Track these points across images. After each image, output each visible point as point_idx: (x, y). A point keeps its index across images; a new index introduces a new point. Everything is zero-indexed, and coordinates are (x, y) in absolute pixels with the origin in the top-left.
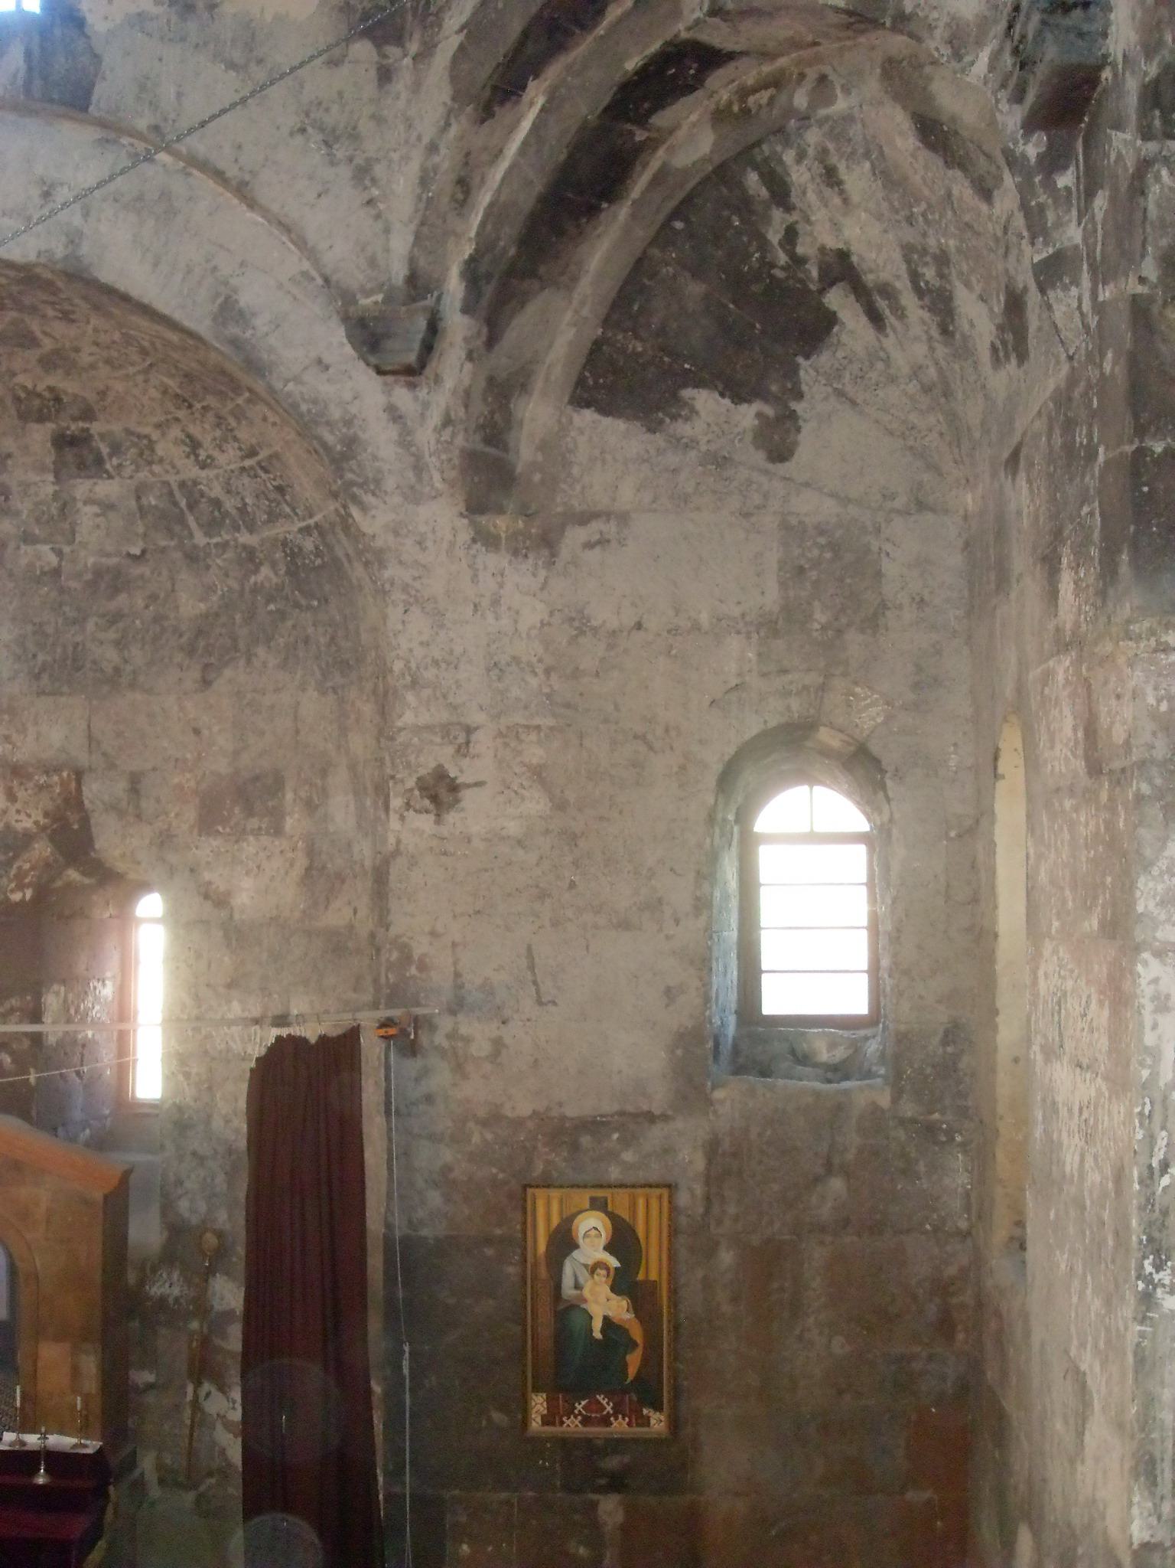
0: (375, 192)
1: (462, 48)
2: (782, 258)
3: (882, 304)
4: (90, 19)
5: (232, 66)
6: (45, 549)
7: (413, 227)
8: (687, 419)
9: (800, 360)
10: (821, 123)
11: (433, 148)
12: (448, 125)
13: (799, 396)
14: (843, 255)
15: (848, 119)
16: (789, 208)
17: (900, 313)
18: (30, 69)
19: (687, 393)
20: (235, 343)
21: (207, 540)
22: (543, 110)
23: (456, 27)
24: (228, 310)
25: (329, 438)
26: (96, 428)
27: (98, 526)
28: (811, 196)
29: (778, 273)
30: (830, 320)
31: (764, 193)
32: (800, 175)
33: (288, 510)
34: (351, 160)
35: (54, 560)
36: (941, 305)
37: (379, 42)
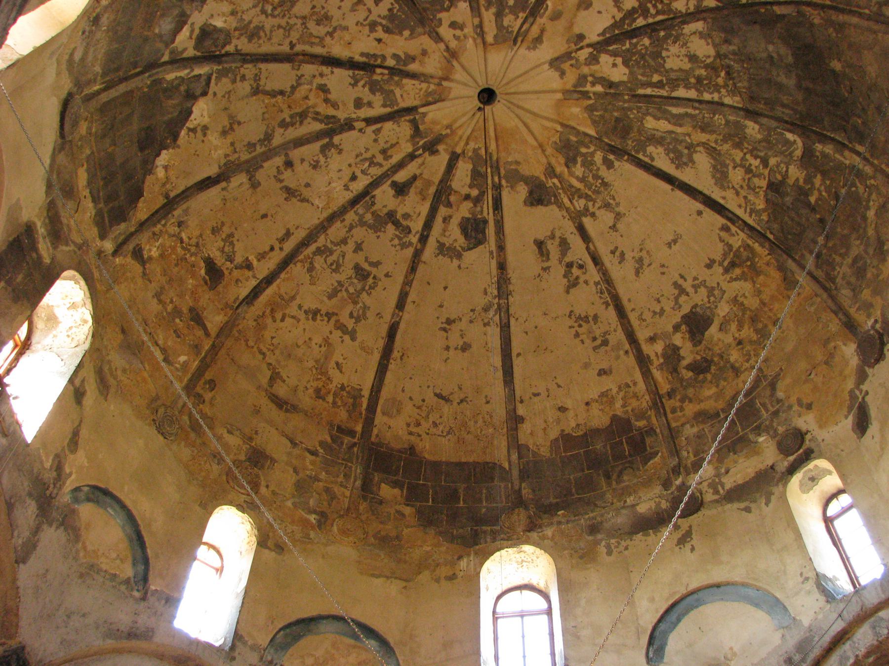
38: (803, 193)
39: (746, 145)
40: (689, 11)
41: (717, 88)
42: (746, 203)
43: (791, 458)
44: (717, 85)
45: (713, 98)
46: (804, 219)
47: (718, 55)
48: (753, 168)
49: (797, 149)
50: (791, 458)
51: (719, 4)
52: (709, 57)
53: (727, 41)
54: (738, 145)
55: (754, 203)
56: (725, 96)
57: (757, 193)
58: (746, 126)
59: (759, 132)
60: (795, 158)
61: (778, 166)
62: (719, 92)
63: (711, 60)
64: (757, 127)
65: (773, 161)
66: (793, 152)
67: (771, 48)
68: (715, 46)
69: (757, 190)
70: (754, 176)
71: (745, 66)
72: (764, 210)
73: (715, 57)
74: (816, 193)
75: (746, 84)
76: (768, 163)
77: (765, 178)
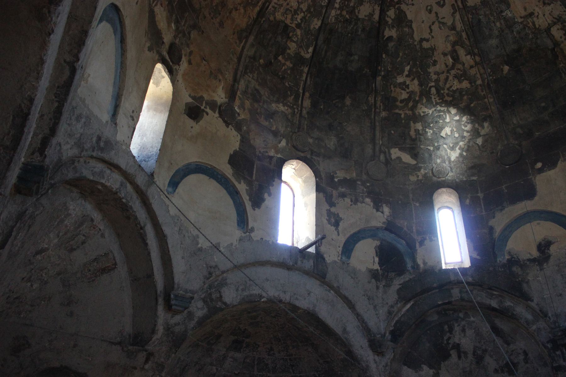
0: (377, 312)
1: (400, 288)
2: (445, 342)
3: (462, 355)
4: (326, 259)
5: (352, 278)
6: (214, 368)
7: (387, 322)
8: (422, 371)
9: (442, 362)
10: (466, 321)
11: (392, 306)
12: (397, 303)
13: (440, 369)
14: (458, 345)
15: (474, 322)
16: (451, 334)
17: (466, 357)
18: (314, 266)
19: (423, 366)
20: (346, 338)
21: (258, 373)
22: (413, 304)
23: (398, 284)
24: (345, 330)
25: (364, 365)
26: (248, 340)
27: (230, 364)
28: (457, 333)
29: (443, 345)
30: (450, 355)
31: (447, 330)
32: (457, 329)
33: (291, 371)
34: (373, 304)
35: (215, 371)
36: (479, 359)
37: (376, 280)
38: (283, 50)
39: (309, 15)
40: (386, 16)
41: (341, 9)
42: (279, 5)
43: (167, 58)
44: (343, 10)
45: (337, 3)
46: (270, 49)
47: (358, 19)
48: (296, 16)
49: (304, 53)
50: (167, 58)
51: (385, 38)
52: (359, 13)
53: (363, 30)
54: (308, 10)
55: (278, 12)
56: (336, 12)
57: (284, 15)
58: (318, 19)
59: (314, 28)
60: (300, 50)
61: (297, 36)
62: (339, 9)
63: (357, 13)
64: (317, 27)
65: (299, 32)
66: (303, 49)
67: (356, 57)
68: (363, 19)
69: (285, 16)
70: (292, 15)
71: (349, 35)
72: (275, 18)
73: (357, 17)
74: (283, 61)
75: (340, 30)
76: (298, 29)
77: (291, 23)
